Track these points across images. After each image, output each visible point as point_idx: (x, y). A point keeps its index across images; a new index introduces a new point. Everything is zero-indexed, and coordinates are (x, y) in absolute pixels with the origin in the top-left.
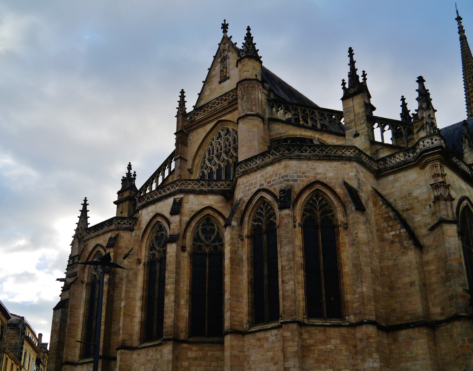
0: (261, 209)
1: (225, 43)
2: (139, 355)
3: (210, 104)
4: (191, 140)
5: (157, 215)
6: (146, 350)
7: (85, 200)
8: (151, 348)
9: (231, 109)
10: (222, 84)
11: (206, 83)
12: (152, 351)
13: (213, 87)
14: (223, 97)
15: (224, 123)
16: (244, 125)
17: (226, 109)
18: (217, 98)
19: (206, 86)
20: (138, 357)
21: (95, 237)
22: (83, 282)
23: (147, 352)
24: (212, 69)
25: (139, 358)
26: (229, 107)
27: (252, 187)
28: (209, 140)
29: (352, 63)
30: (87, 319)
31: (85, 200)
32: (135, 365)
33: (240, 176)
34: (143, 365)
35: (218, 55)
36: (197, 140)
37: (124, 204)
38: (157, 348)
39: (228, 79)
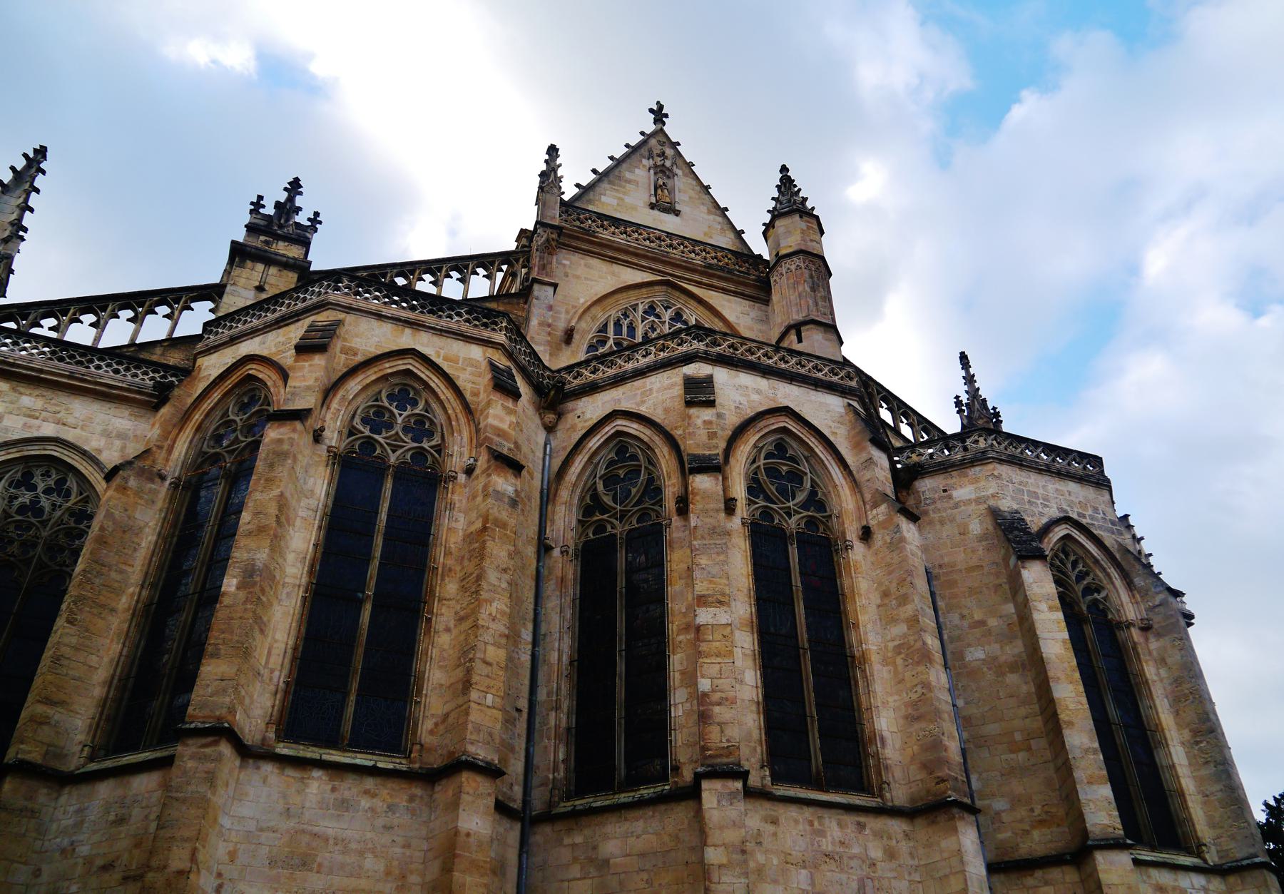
0: (1061, 561)
1: (664, 142)
2: (775, 822)
3: (644, 230)
4: (564, 265)
5: (787, 411)
6: (808, 812)
7: (42, 152)
8: (833, 811)
9: (705, 280)
10: (656, 212)
11: (606, 179)
12: (840, 825)
13: (628, 200)
14: (686, 243)
15: (677, 294)
16: (827, 343)
17: (694, 271)
18: (668, 233)
19: (605, 185)
20: (771, 828)
21: (395, 320)
22: (318, 437)
23: (816, 824)
24: (624, 166)
25: (775, 834)
26: (702, 273)
27: (1039, 502)
28: (625, 301)
29: (970, 379)
30: (315, 582)
31: (42, 152)
32: (761, 858)
33: (1001, 460)
34: (804, 867)
35: (644, 151)
36: (586, 279)
37: (273, 270)
38: (862, 819)
39: (677, 215)
